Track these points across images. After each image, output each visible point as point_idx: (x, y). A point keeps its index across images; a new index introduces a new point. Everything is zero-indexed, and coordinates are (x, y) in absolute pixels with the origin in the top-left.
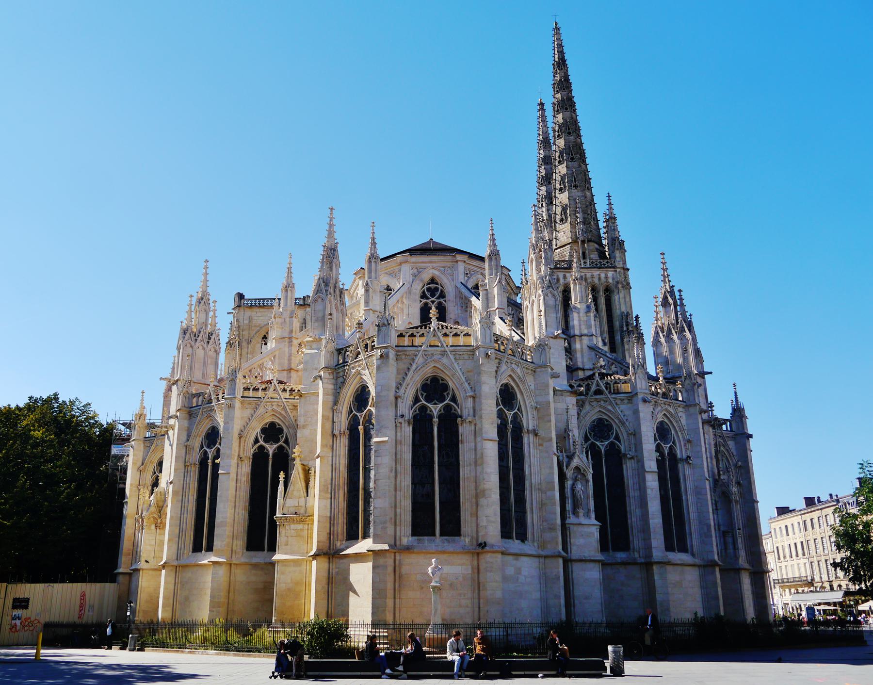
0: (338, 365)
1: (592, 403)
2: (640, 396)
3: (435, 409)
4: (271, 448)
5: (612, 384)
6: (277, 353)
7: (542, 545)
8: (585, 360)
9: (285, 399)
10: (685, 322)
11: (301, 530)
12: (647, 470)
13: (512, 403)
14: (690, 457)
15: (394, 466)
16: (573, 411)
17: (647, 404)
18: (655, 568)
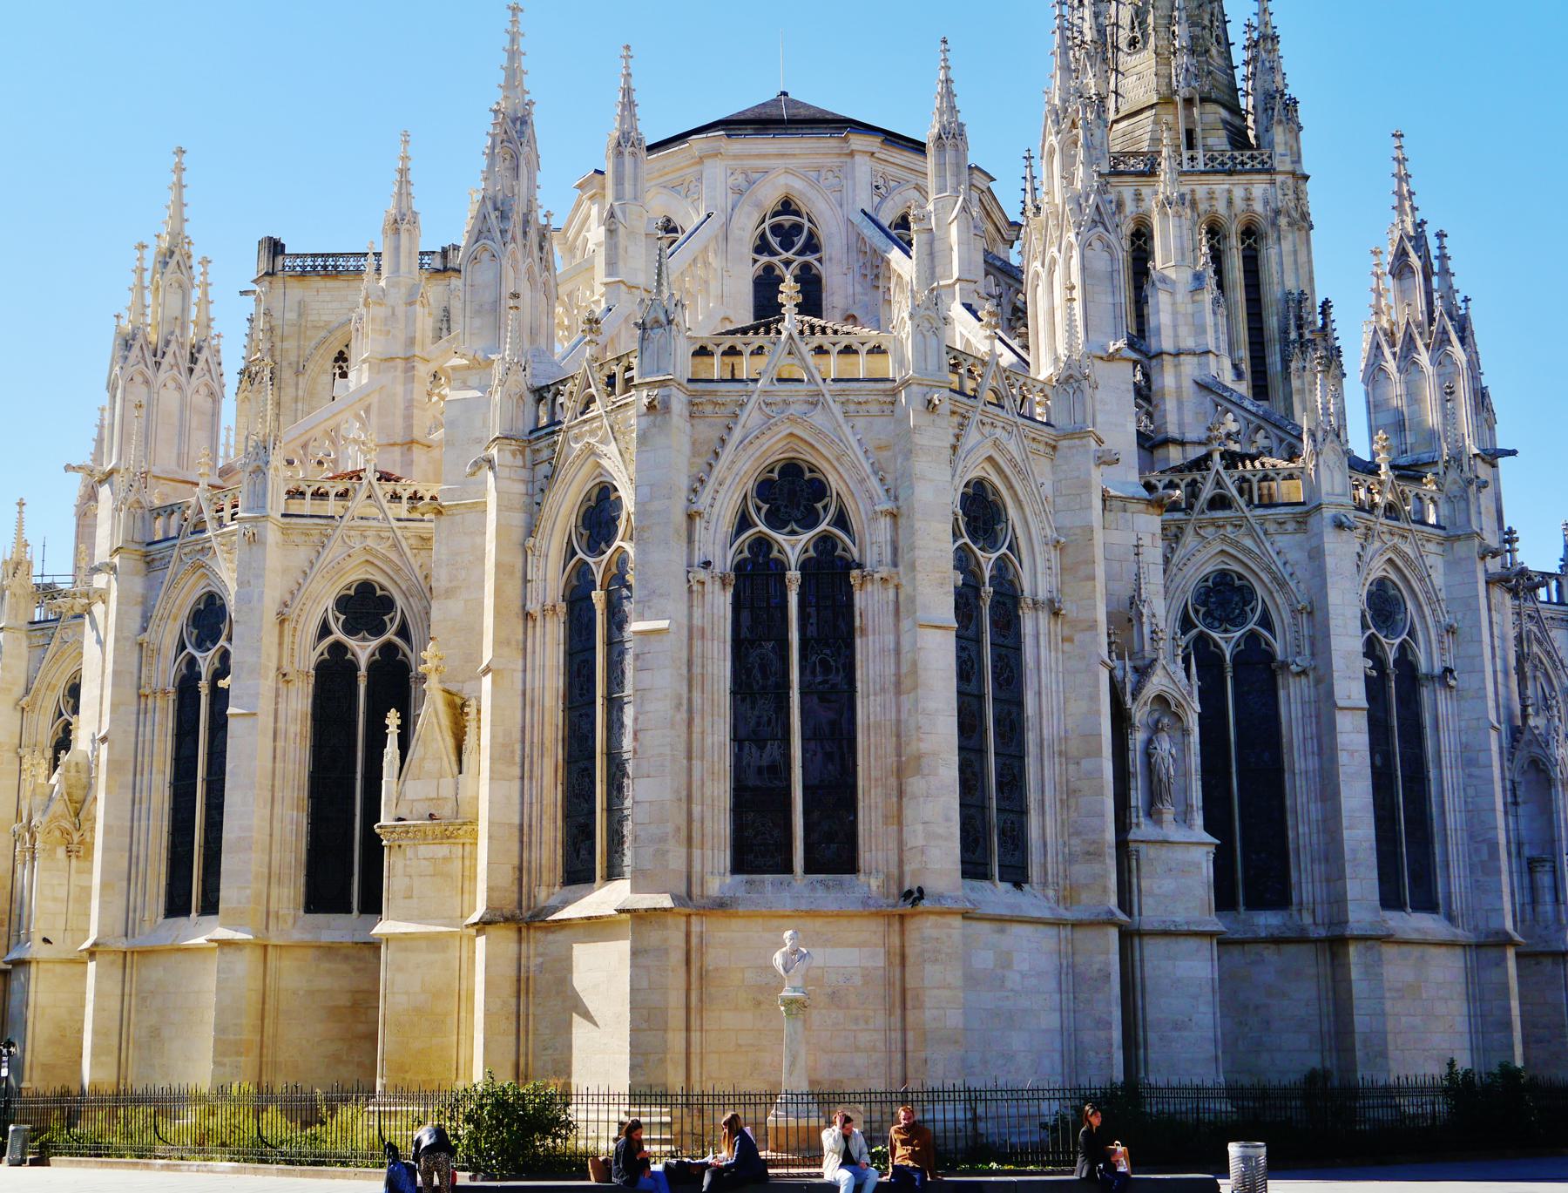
0: (537, 429)
1: (1202, 532)
2: (1328, 513)
3: (793, 547)
4: (363, 650)
5: (1255, 480)
6: (374, 399)
7: (1068, 896)
9: (399, 520)
10: (1451, 318)
11: (445, 859)
12: (1340, 703)
13: (994, 531)
14: (1451, 671)
15: (685, 696)
16: (1154, 552)
17: (1346, 534)
18: (1353, 951)
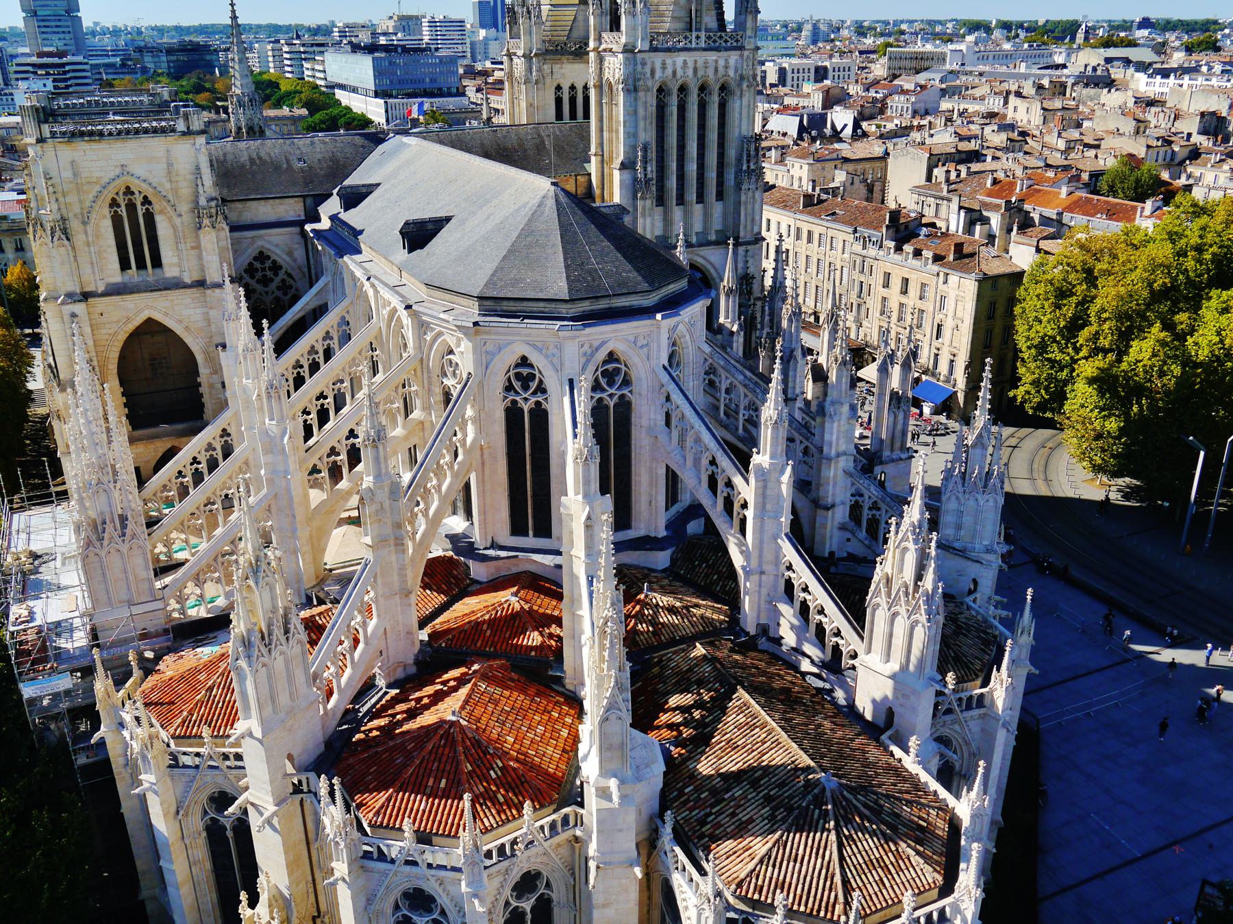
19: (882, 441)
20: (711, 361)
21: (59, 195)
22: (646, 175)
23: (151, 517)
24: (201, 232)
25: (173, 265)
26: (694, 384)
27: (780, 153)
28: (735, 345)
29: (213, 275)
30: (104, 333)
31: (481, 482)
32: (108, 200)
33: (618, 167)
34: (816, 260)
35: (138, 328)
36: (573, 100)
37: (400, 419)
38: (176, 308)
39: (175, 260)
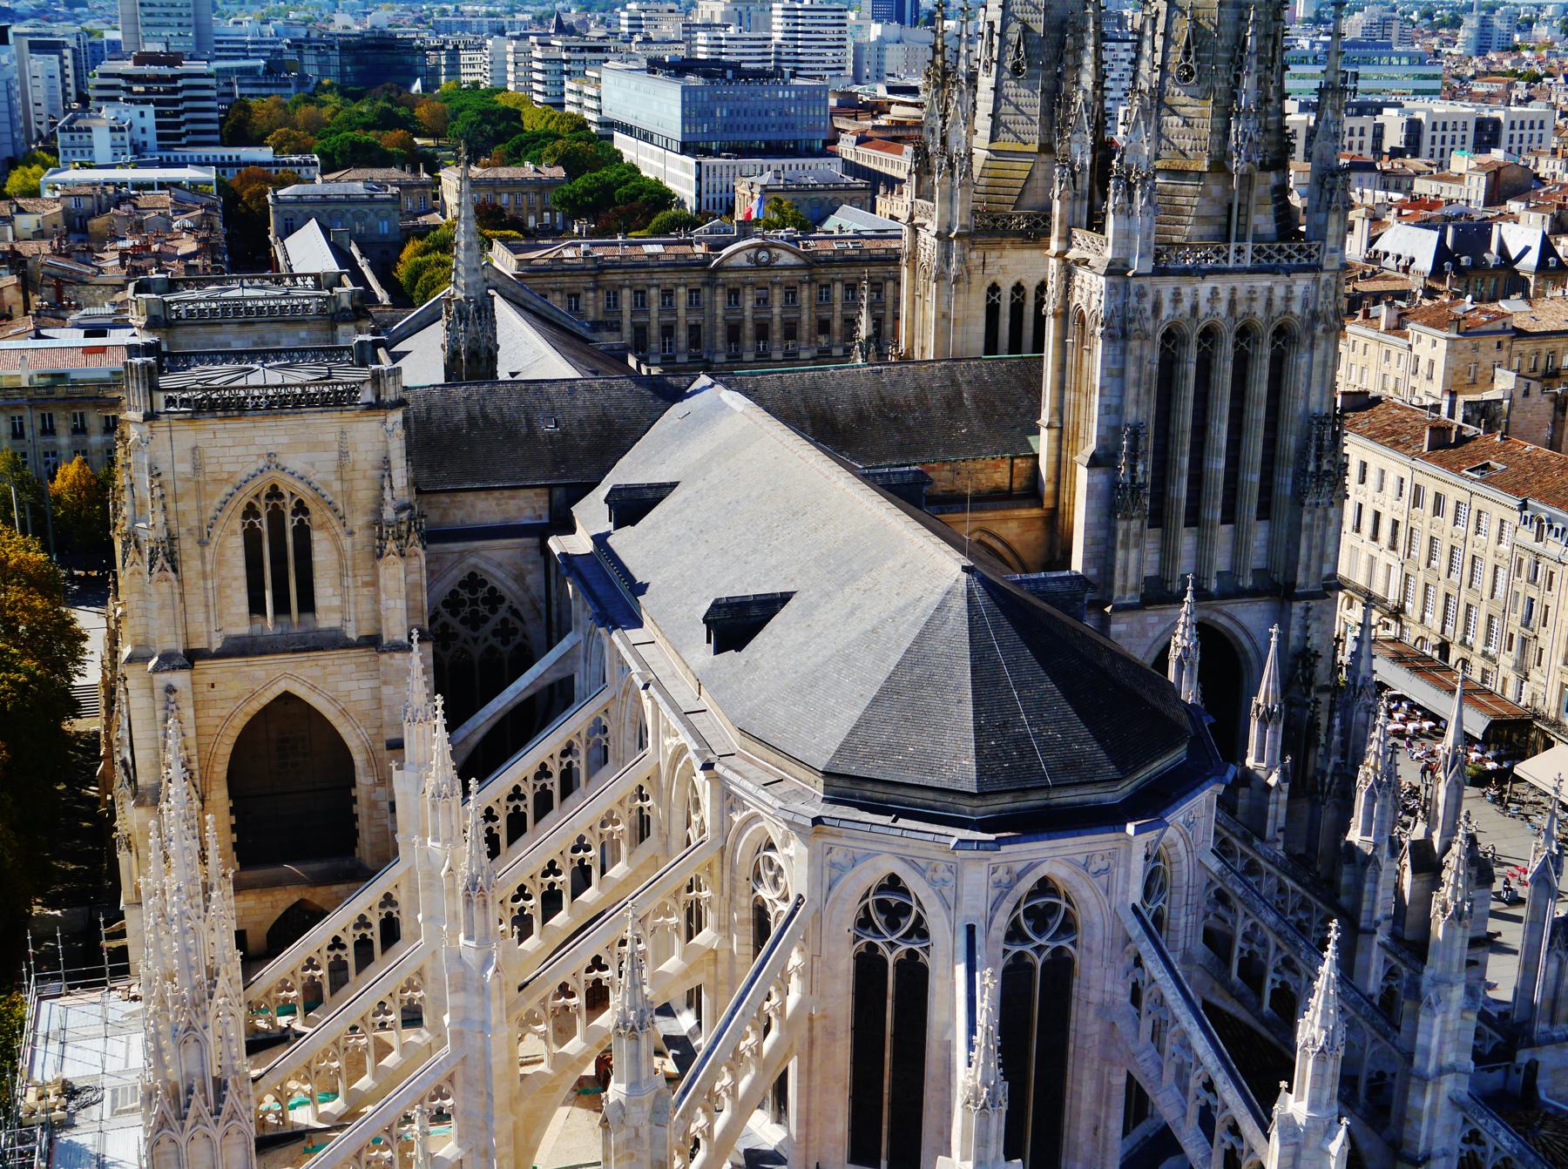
8: (1437, 1133)
19: (1533, 1007)
20: (1219, 885)
21: (169, 499)
22: (1133, 479)
23: (257, 1030)
24: (381, 564)
25: (329, 609)
26: (1185, 924)
27: (1396, 312)
28: (1271, 808)
29: (396, 627)
30: (213, 715)
31: (806, 1072)
32: (242, 507)
33: (1086, 461)
34: (1447, 548)
35: (266, 709)
36: (1017, 309)
37: (678, 943)
38: (330, 679)
39: (336, 602)
